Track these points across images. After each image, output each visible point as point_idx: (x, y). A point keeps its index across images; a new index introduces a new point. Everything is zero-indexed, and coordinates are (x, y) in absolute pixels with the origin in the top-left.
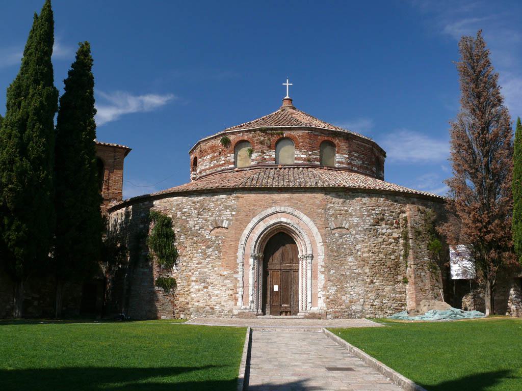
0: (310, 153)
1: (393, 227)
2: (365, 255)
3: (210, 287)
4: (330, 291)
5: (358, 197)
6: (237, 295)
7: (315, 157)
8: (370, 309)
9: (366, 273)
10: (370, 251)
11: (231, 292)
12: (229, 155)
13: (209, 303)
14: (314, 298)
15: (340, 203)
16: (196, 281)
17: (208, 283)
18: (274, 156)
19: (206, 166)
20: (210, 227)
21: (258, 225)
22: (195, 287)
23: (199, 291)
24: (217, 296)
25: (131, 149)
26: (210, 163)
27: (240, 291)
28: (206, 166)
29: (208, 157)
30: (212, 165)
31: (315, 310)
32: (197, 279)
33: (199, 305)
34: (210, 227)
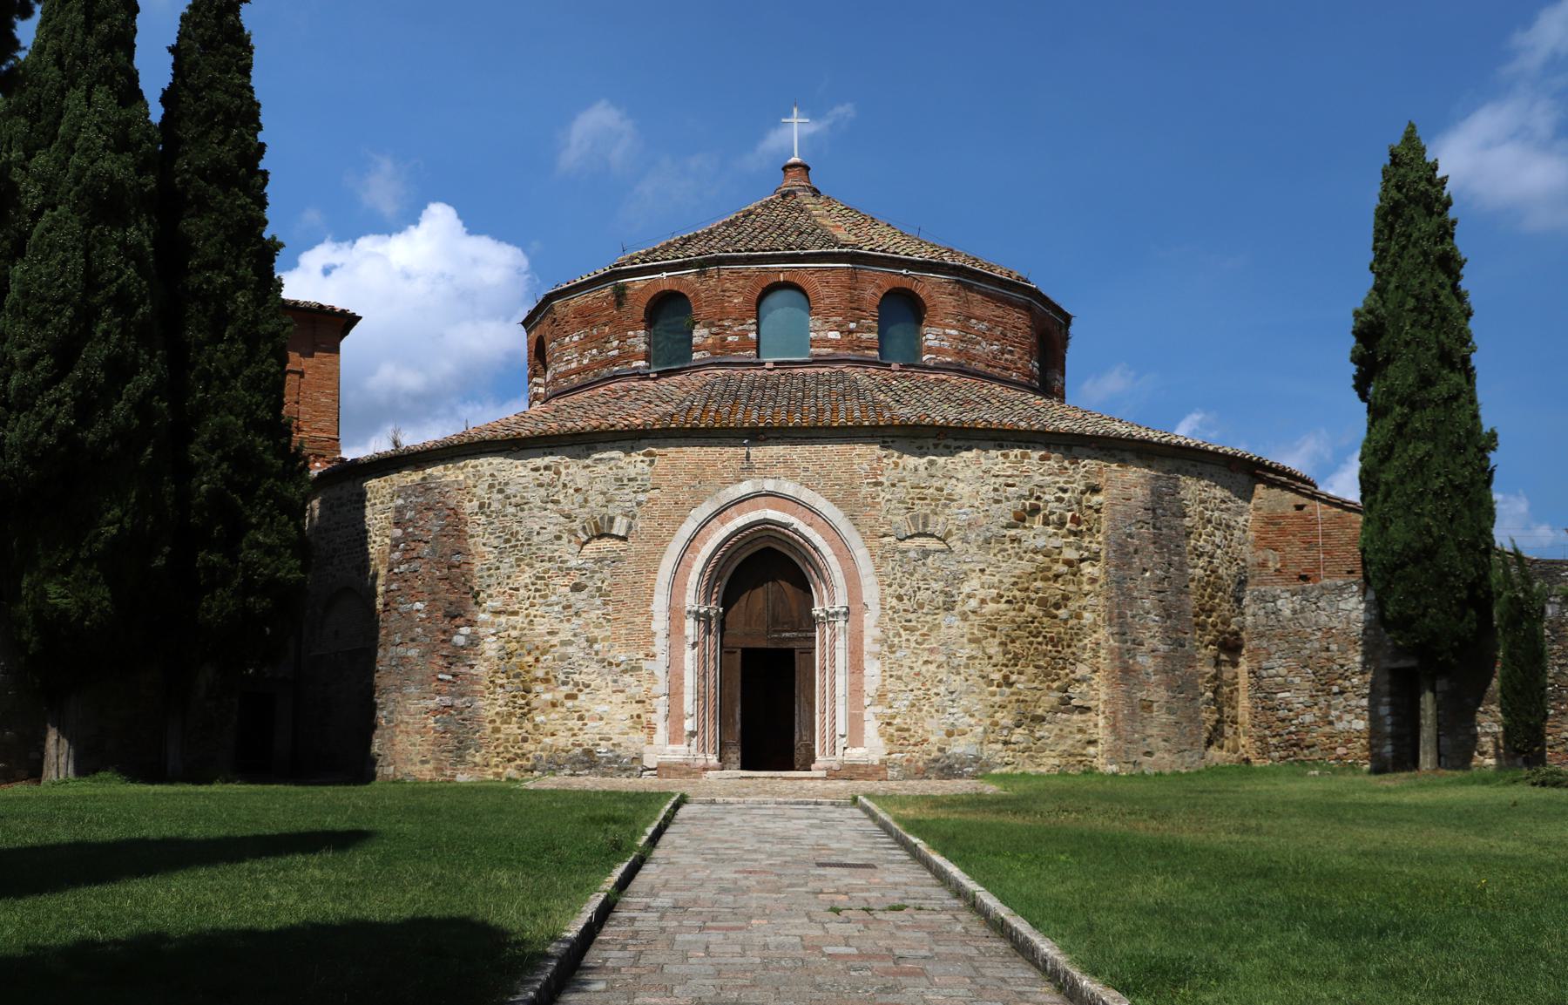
0: (852, 325)
1: (1064, 531)
2: (991, 607)
3: (581, 696)
5: (969, 449)
7: (865, 336)
8: (1003, 754)
9: (990, 658)
10: (1002, 597)
11: (636, 709)
14: (856, 723)
15: (922, 468)
16: (547, 681)
17: (576, 684)
18: (753, 335)
20: (580, 534)
21: (705, 529)
23: (554, 705)
24: (601, 719)
26: (581, 355)
27: (661, 706)
29: (576, 338)
31: (856, 754)
32: (547, 673)
33: (555, 743)
34: (580, 534)
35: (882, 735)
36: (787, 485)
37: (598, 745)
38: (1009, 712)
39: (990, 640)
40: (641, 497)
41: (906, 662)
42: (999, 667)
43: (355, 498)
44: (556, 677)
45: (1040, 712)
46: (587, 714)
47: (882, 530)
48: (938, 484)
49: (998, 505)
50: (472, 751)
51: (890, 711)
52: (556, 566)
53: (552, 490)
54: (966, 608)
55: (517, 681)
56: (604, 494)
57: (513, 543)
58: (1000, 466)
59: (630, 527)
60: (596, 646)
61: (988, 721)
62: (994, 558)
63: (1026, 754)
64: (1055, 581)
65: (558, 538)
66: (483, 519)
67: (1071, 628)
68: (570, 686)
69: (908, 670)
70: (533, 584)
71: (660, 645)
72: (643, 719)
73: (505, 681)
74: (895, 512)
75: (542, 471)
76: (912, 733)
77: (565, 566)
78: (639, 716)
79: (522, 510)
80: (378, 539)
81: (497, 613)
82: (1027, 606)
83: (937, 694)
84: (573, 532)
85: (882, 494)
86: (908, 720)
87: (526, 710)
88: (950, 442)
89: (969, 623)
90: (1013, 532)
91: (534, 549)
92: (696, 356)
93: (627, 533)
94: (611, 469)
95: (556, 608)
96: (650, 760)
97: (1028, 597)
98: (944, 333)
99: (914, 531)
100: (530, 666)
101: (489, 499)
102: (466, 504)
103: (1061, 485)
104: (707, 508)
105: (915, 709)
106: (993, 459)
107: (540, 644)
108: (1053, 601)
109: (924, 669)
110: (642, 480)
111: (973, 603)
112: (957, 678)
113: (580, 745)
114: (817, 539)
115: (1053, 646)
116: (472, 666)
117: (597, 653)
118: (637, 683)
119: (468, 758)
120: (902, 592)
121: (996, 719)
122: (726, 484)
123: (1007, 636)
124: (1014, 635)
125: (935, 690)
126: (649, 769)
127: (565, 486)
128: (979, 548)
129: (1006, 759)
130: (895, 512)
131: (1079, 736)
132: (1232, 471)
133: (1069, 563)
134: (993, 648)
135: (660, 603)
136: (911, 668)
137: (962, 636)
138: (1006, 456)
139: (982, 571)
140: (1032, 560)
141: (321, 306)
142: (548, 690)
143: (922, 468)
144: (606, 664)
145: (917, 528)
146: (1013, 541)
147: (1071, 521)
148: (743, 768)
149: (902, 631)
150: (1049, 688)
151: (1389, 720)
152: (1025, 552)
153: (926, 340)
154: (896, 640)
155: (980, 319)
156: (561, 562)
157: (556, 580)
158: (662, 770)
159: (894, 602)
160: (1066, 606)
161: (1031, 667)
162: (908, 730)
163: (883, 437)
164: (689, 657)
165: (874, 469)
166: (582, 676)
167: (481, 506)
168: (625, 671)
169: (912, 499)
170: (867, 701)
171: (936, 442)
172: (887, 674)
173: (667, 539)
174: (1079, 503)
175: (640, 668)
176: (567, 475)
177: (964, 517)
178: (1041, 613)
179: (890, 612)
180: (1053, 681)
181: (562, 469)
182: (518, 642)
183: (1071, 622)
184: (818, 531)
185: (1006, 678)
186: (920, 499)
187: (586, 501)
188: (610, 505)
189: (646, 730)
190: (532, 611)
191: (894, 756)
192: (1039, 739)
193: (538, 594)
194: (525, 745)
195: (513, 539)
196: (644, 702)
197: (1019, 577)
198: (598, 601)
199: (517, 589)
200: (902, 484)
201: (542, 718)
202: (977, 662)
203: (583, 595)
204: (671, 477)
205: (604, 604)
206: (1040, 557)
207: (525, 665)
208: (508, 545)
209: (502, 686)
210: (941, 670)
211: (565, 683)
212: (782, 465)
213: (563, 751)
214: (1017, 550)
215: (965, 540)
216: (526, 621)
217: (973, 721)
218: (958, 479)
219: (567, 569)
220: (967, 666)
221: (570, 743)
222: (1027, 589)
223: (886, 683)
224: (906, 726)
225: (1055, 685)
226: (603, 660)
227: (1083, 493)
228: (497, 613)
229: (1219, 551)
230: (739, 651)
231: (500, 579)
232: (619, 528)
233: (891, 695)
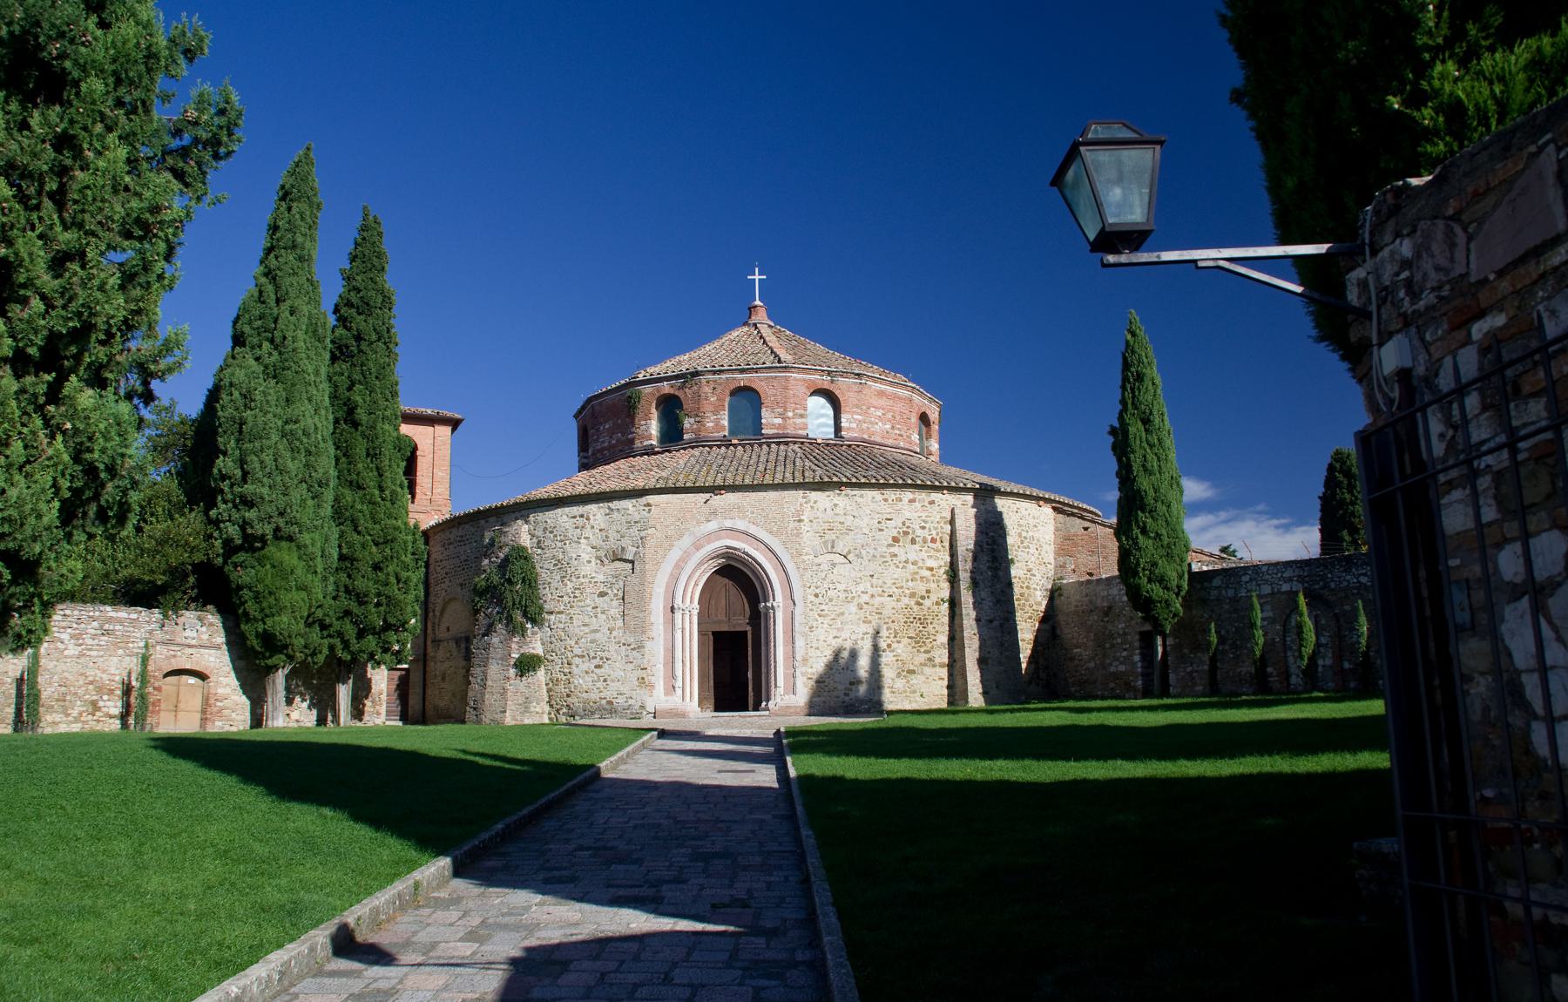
3: (606, 666)
13: (602, 695)
17: (602, 659)
19: (603, 442)
22: (581, 666)
26: (611, 437)
28: (603, 442)
29: (607, 426)
30: (613, 442)
41: (822, 638)
45: (912, 667)
65: (589, 562)
77: (593, 580)
84: (597, 558)
90: (892, 550)
92: (686, 437)
104: (686, 541)
116: (533, 648)
119: (532, 709)
120: (818, 591)
122: (699, 522)
127: (593, 527)
133: (931, 569)
138: (886, 500)
139: (872, 576)
150: (918, 651)
151: (1139, 665)
159: (812, 598)
167: (539, 542)
178: (913, 603)
181: (591, 517)
190: (572, 611)
206: (910, 566)
211: (594, 658)
225: (922, 650)
226: (619, 643)
229: (1033, 559)
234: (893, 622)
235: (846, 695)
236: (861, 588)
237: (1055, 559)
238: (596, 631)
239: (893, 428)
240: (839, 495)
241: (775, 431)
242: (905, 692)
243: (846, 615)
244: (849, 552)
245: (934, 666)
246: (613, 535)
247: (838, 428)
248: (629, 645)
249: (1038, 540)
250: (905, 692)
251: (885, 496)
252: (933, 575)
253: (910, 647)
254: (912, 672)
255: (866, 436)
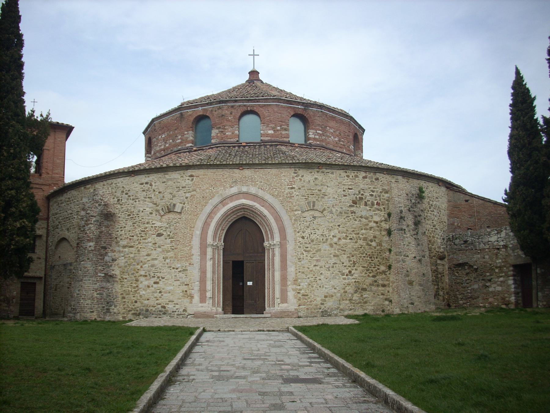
0: (279, 128)
3: (161, 283)
4: (302, 284)
6: (193, 291)
8: (349, 305)
9: (343, 263)
10: (348, 236)
11: (185, 288)
12: (186, 133)
14: (284, 293)
15: (312, 182)
16: (146, 276)
17: (158, 277)
19: (160, 146)
20: (161, 212)
23: (149, 287)
24: (169, 293)
25: (74, 127)
26: (166, 143)
27: (196, 286)
28: (160, 146)
29: (163, 136)
30: (167, 145)
31: (284, 306)
32: (146, 273)
34: (161, 212)
35: (296, 298)
36: (252, 189)
37: (168, 304)
38: (351, 286)
39: (343, 255)
40: (188, 195)
41: (306, 266)
42: (347, 267)
43: (67, 200)
44: (149, 275)
45: (365, 286)
46: (163, 291)
47: (295, 208)
48: (319, 188)
49: (345, 198)
50: (113, 307)
51: (299, 287)
52: (150, 226)
53: (149, 193)
54: (332, 242)
55: (133, 276)
56: (171, 194)
57: (132, 216)
58: (346, 181)
59: (183, 208)
60: (168, 261)
61: (342, 291)
62: (344, 220)
63: (360, 305)
64: (370, 230)
65: (151, 213)
66: (119, 206)
67: (378, 250)
68: (156, 278)
69: (307, 269)
70: (140, 234)
71: (196, 258)
72: (188, 293)
73: (128, 276)
74: (301, 200)
75: (144, 185)
76: (309, 297)
77: (153, 226)
78: (186, 291)
79: (136, 202)
80: (76, 217)
81: (124, 247)
82: (359, 241)
83: (320, 279)
84: (157, 211)
85: (295, 193)
86: (307, 291)
87: (136, 289)
88: (324, 170)
89: (333, 248)
90: (352, 209)
91: (140, 219)
93: (181, 211)
94: (174, 183)
95: (150, 244)
96: (191, 310)
97: (359, 237)
98: (316, 132)
99: (309, 209)
100: (138, 270)
101: (121, 197)
102: (112, 200)
103: (372, 189)
104: (216, 200)
105: (310, 286)
106: (342, 177)
107: (143, 260)
108: (370, 239)
109: (314, 268)
110: (188, 187)
111: (335, 240)
112: (329, 272)
113: (160, 304)
114: (265, 212)
115: (370, 258)
117: (167, 264)
118: (185, 277)
119: (111, 310)
121: (346, 290)
123: (350, 253)
124: (353, 253)
125: (319, 278)
126: (191, 315)
127: (154, 190)
128: (337, 215)
129: (350, 307)
130: (301, 200)
131: (382, 297)
132: (440, 186)
133: (377, 223)
134: (344, 258)
135: (196, 242)
136: (309, 268)
137: (331, 254)
138: (348, 176)
139: (339, 226)
140: (360, 221)
141: (58, 123)
142: (146, 280)
143: (312, 182)
144: (171, 268)
145: (310, 207)
146: (352, 213)
147: (376, 205)
148: (233, 313)
149: (304, 252)
152: (357, 217)
153: (309, 135)
154: (302, 257)
155: (331, 128)
156: (153, 224)
157: (150, 232)
158: (196, 315)
159: (301, 239)
160: (375, 241)
161: (361, 267)
162: (307, 295)
163: (295, 168)
164: (209, 264)
165: (291, 182)
166: (161, 274)
167: (118, 200)
168: (180, 271)
169: (308, 194)
170: (289, 283)
171: (318, 170)
172: (298, 271)
173: (199, 213)
174: (379, 196)
175: (187, 270)
176: (155, 186)
177: (331, 202)
178: (365, 244)
179: (299, 244)
180: (370, 273)
181: (153, 184)
182: (133, 259)
183: (378, 248)
184: (266, 209)
185: (350, 272)
186: (311, 194)
187: (163, 197)
188: (174, 198)
189: (189, 297)
191: (301, 307)
192: (365, 298)
193: (142, 238)
194: (136, 304)
195: (131, 215)
196: (188, 285)
197: (355, 228)
198: (169, 241)
199: (133, 236)
200: (304, 188)
201: (144, 292)
202: (337, 265)
203: (162, 237)
204: (201, 186)
205: (171, 242)
207: (136, 269)
208: (129, 217)
209: (126, 279)
210: (321, 269)
211: (154, 277)
212: (250, 180)
213: (153, 307)
214: (354, 217)
215: (331, 212)
216: (137, 250)
217: (336, 291)
218: (328, 186)
219: (155, 227)
220: (333, 267)
221: (155, 304)
222: (358, 234)
223: (297, 275)
224: (306, 294)
225: (371, 275)
226: (170, 267)
227: (381, 192)
228: (124, 247)
229: (436, 218)
230: (231, 262)
231: (126, 232)
232: (178, 209)
233: (299, 280)
234: (353, 256)
235: (322, 304)
236: (332, 234)
237: (448, 220)
238: (156, 259)
239: (340, 141)
240: (318, 172)
241: (269, 138)
242: (360, 303)
243: (322, 251)
244: (324, 210)
245: (378, 286)
246: (168, 196)
247: (307, 138)
248: (177, 269)
249: (439, 208)
250: (360, 303)
251: (348, 174)
252: (378, 227)
253: (364, 273)
254: (364, 290)
255: (324, 144)
